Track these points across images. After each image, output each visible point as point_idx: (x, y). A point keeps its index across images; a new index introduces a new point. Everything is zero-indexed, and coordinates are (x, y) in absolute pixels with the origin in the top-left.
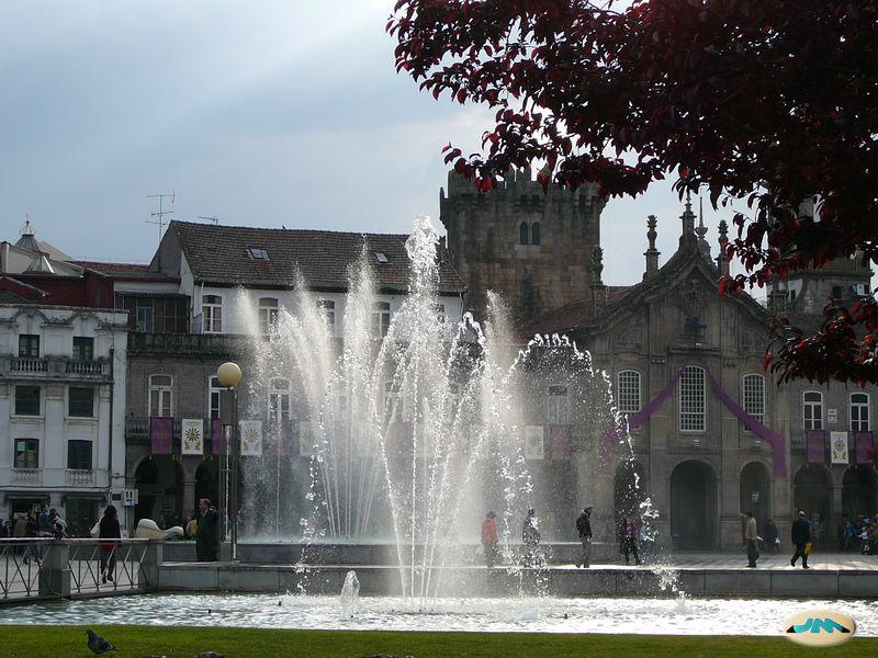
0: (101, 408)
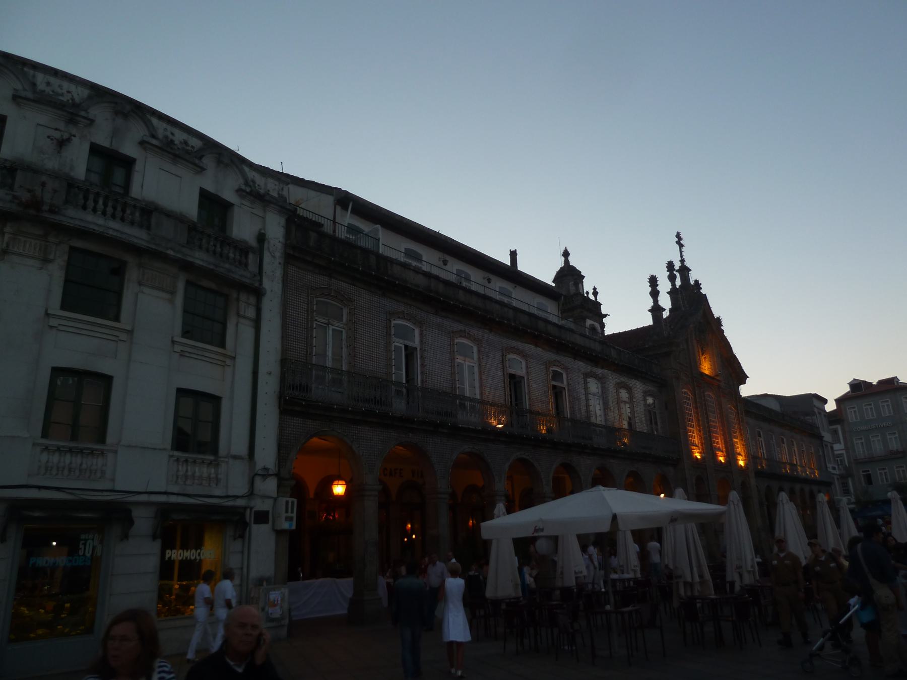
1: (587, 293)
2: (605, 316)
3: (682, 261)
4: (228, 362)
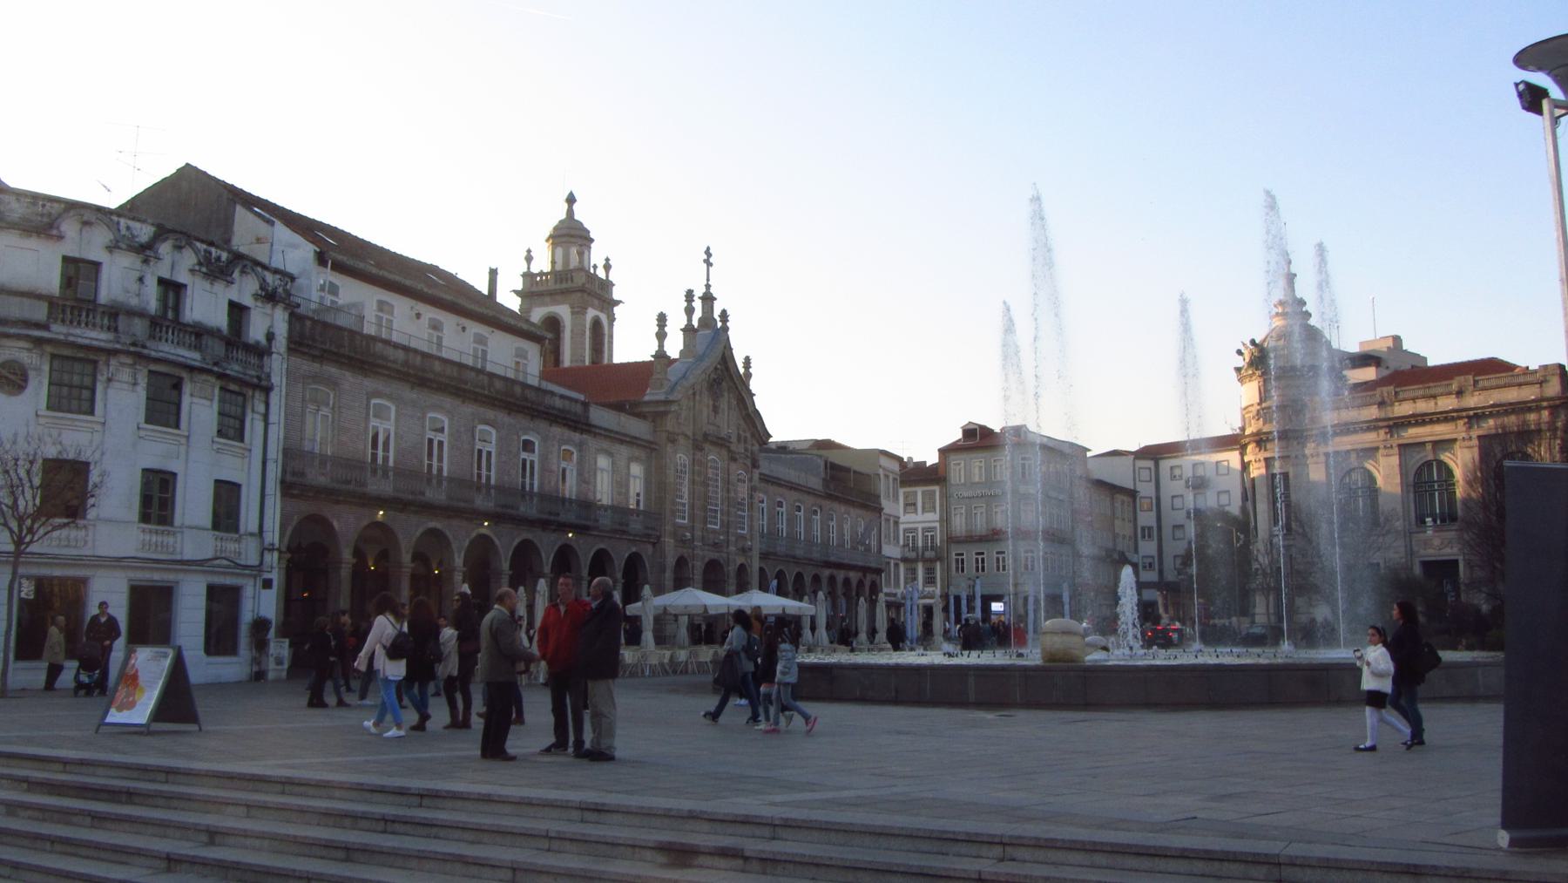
0: (254, 426)
1: (595, 267)
2: (618, 302)
3: (708, 286)
4: (247, 454)
